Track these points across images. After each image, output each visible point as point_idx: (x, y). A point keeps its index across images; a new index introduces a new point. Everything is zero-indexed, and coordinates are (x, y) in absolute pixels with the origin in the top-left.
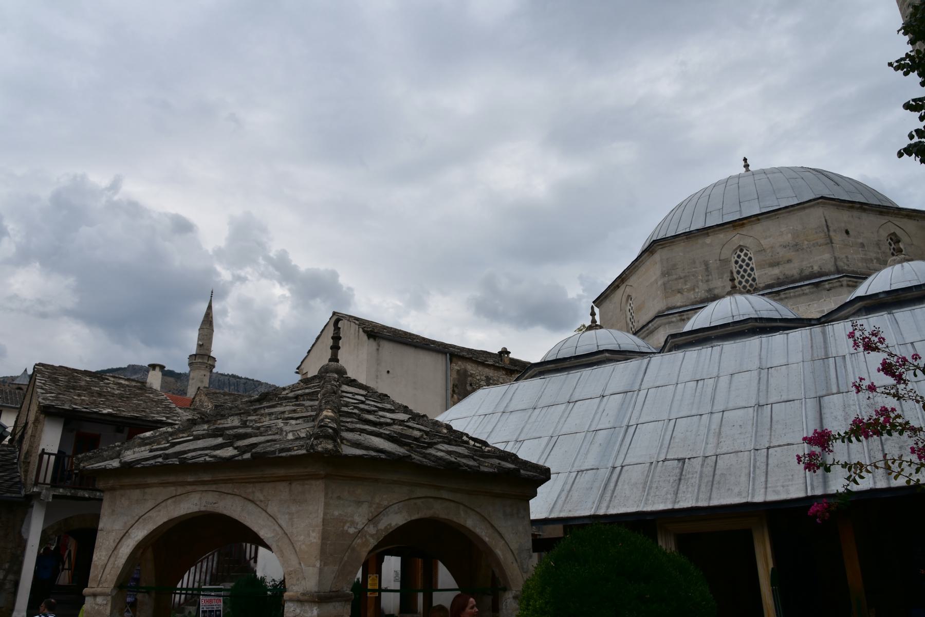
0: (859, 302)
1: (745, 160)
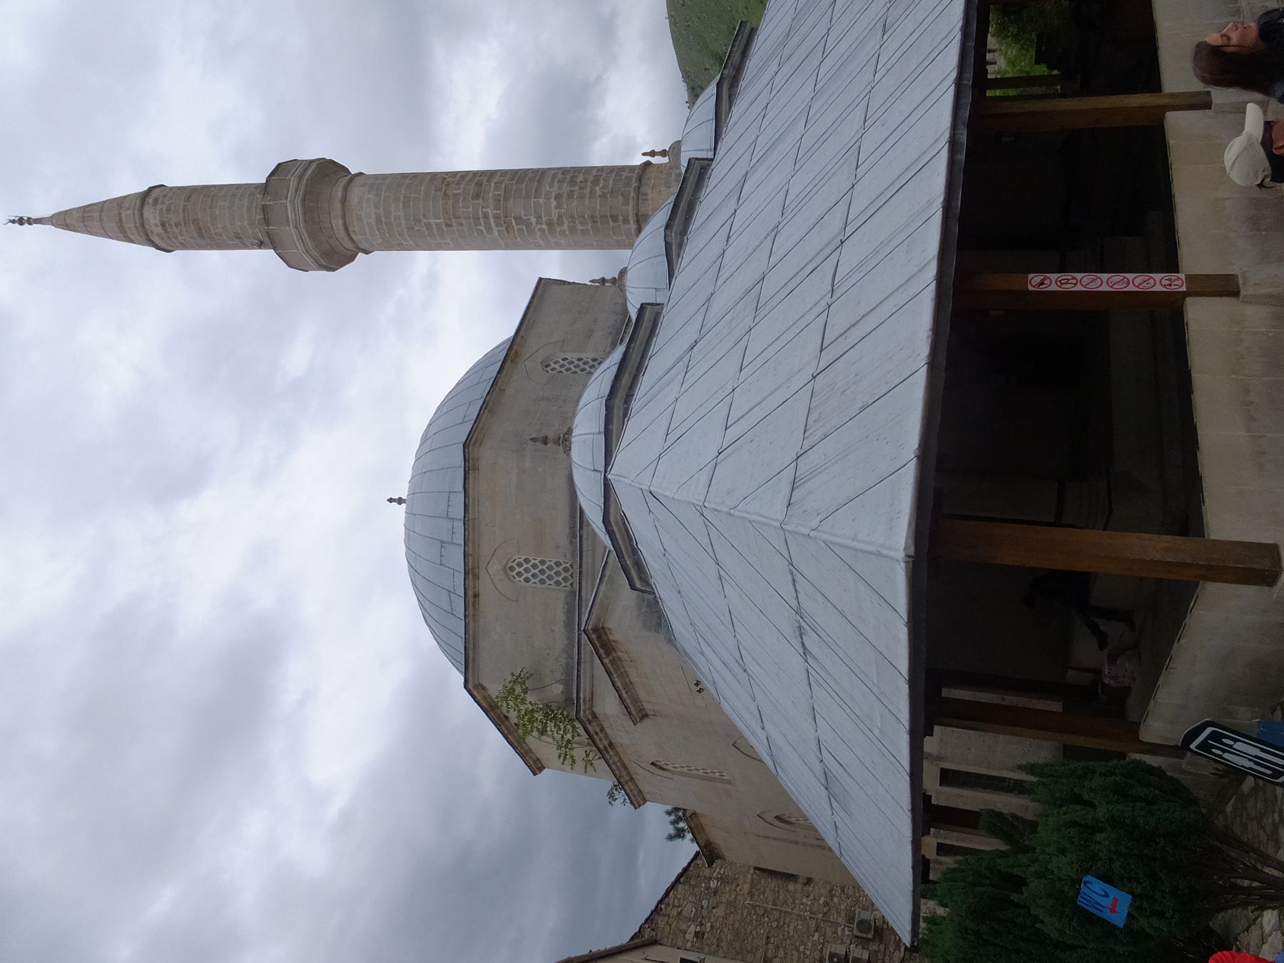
0: (722, 87)
1: (391, 500)
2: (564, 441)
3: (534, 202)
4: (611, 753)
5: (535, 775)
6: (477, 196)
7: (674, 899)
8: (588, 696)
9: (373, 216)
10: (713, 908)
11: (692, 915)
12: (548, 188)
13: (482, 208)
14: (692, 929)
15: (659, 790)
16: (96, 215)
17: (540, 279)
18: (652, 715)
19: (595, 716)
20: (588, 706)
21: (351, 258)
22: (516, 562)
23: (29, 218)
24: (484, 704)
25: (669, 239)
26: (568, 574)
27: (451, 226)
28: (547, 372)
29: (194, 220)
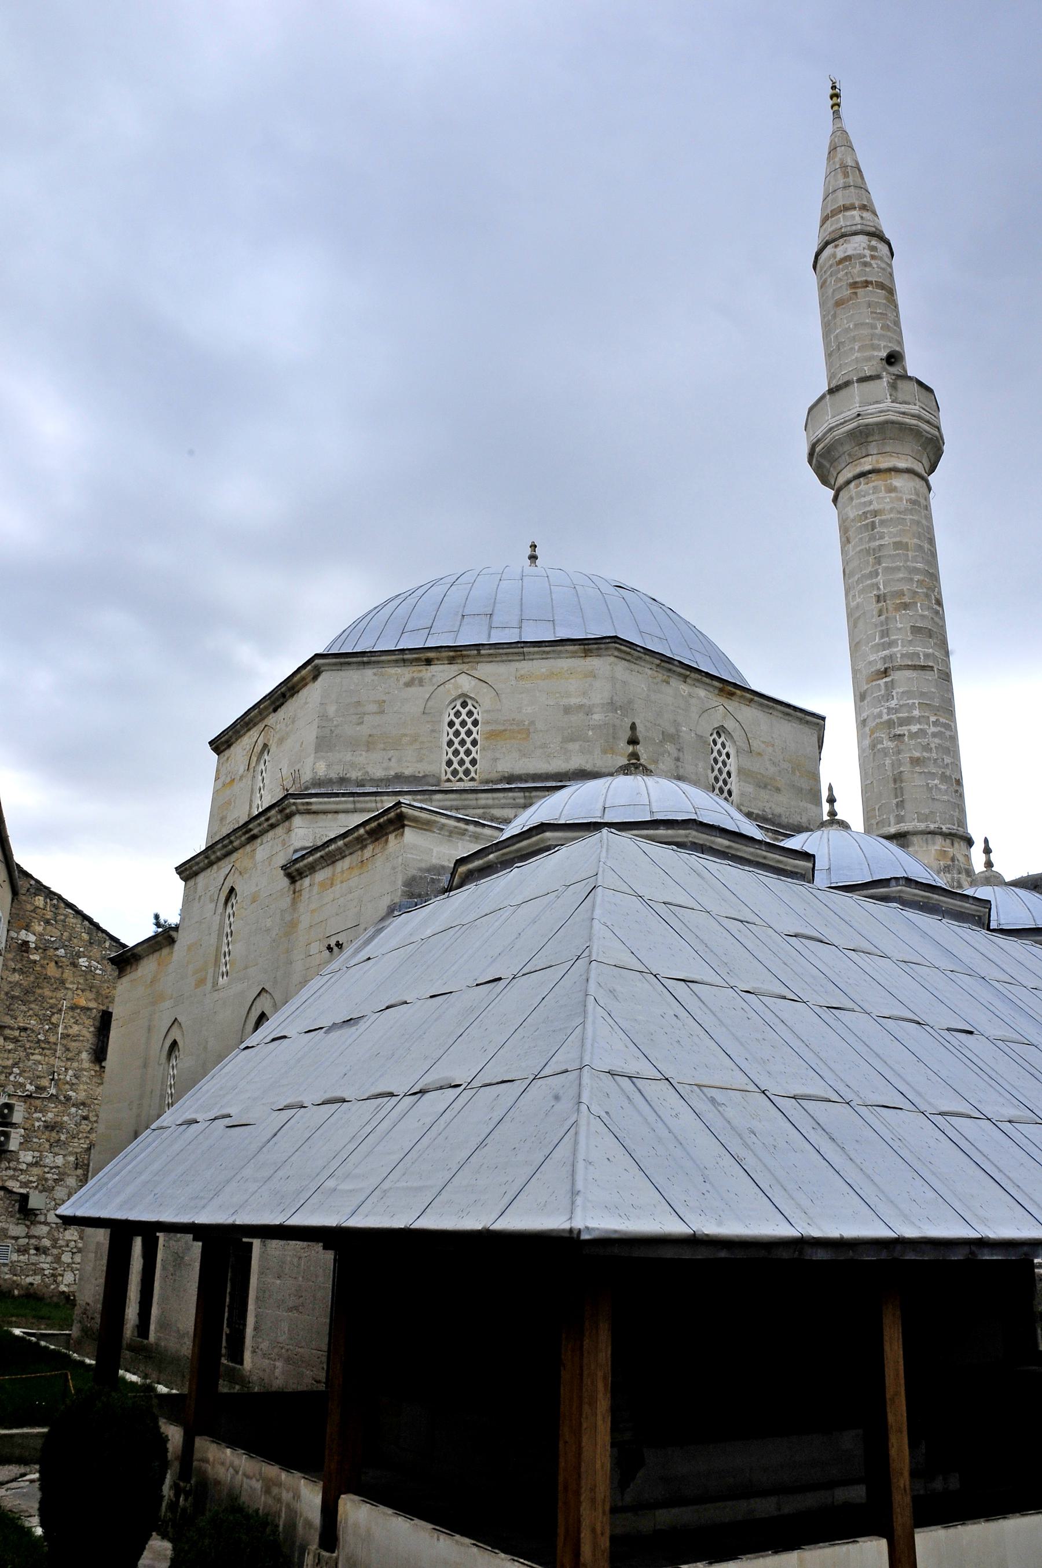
1: (534, 546)
2: (634, 766)
3: (914, 703)
4: (243, 838)
5: (210, 743)
6: (916, 630)
7: (64, 915)
8: (314, 808)
9: (881, 506)
10: (56, 963)
11: (46, 937)
12: (933, 719)
13: (902, 639)
14: (32, 938)
15: (200, 897)
16: (851, 180)
17: (823, 719)
18: (295, 889)
19: (289, 817)
20: (301, 807)
21: (825, 481)
22: (473, 709)
23: (838, 105)
24: (296, 679)
25: (893, 882)
26: (461, 775)
27: (878, 601)
28: (711, 735)
29: (856, 293)
